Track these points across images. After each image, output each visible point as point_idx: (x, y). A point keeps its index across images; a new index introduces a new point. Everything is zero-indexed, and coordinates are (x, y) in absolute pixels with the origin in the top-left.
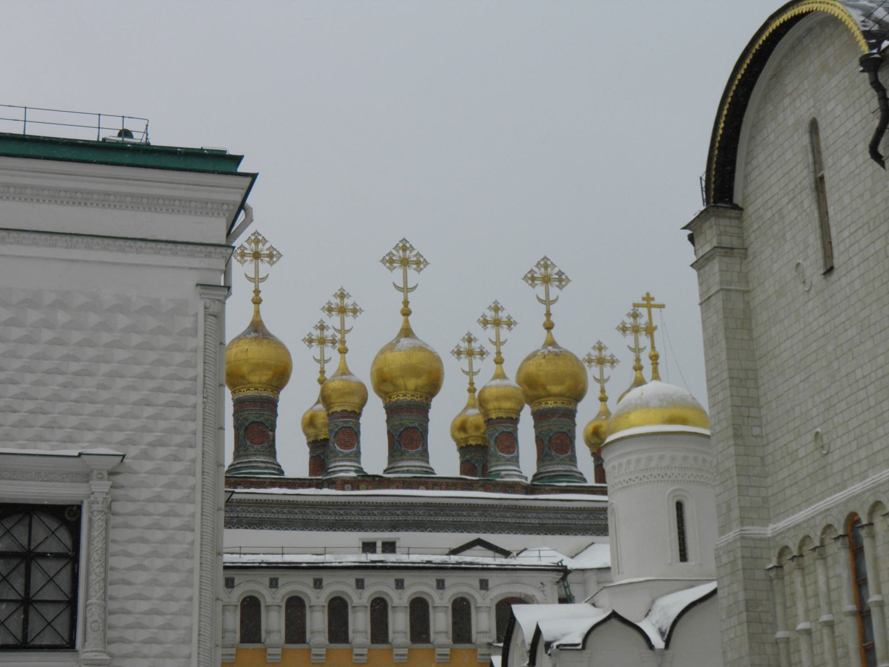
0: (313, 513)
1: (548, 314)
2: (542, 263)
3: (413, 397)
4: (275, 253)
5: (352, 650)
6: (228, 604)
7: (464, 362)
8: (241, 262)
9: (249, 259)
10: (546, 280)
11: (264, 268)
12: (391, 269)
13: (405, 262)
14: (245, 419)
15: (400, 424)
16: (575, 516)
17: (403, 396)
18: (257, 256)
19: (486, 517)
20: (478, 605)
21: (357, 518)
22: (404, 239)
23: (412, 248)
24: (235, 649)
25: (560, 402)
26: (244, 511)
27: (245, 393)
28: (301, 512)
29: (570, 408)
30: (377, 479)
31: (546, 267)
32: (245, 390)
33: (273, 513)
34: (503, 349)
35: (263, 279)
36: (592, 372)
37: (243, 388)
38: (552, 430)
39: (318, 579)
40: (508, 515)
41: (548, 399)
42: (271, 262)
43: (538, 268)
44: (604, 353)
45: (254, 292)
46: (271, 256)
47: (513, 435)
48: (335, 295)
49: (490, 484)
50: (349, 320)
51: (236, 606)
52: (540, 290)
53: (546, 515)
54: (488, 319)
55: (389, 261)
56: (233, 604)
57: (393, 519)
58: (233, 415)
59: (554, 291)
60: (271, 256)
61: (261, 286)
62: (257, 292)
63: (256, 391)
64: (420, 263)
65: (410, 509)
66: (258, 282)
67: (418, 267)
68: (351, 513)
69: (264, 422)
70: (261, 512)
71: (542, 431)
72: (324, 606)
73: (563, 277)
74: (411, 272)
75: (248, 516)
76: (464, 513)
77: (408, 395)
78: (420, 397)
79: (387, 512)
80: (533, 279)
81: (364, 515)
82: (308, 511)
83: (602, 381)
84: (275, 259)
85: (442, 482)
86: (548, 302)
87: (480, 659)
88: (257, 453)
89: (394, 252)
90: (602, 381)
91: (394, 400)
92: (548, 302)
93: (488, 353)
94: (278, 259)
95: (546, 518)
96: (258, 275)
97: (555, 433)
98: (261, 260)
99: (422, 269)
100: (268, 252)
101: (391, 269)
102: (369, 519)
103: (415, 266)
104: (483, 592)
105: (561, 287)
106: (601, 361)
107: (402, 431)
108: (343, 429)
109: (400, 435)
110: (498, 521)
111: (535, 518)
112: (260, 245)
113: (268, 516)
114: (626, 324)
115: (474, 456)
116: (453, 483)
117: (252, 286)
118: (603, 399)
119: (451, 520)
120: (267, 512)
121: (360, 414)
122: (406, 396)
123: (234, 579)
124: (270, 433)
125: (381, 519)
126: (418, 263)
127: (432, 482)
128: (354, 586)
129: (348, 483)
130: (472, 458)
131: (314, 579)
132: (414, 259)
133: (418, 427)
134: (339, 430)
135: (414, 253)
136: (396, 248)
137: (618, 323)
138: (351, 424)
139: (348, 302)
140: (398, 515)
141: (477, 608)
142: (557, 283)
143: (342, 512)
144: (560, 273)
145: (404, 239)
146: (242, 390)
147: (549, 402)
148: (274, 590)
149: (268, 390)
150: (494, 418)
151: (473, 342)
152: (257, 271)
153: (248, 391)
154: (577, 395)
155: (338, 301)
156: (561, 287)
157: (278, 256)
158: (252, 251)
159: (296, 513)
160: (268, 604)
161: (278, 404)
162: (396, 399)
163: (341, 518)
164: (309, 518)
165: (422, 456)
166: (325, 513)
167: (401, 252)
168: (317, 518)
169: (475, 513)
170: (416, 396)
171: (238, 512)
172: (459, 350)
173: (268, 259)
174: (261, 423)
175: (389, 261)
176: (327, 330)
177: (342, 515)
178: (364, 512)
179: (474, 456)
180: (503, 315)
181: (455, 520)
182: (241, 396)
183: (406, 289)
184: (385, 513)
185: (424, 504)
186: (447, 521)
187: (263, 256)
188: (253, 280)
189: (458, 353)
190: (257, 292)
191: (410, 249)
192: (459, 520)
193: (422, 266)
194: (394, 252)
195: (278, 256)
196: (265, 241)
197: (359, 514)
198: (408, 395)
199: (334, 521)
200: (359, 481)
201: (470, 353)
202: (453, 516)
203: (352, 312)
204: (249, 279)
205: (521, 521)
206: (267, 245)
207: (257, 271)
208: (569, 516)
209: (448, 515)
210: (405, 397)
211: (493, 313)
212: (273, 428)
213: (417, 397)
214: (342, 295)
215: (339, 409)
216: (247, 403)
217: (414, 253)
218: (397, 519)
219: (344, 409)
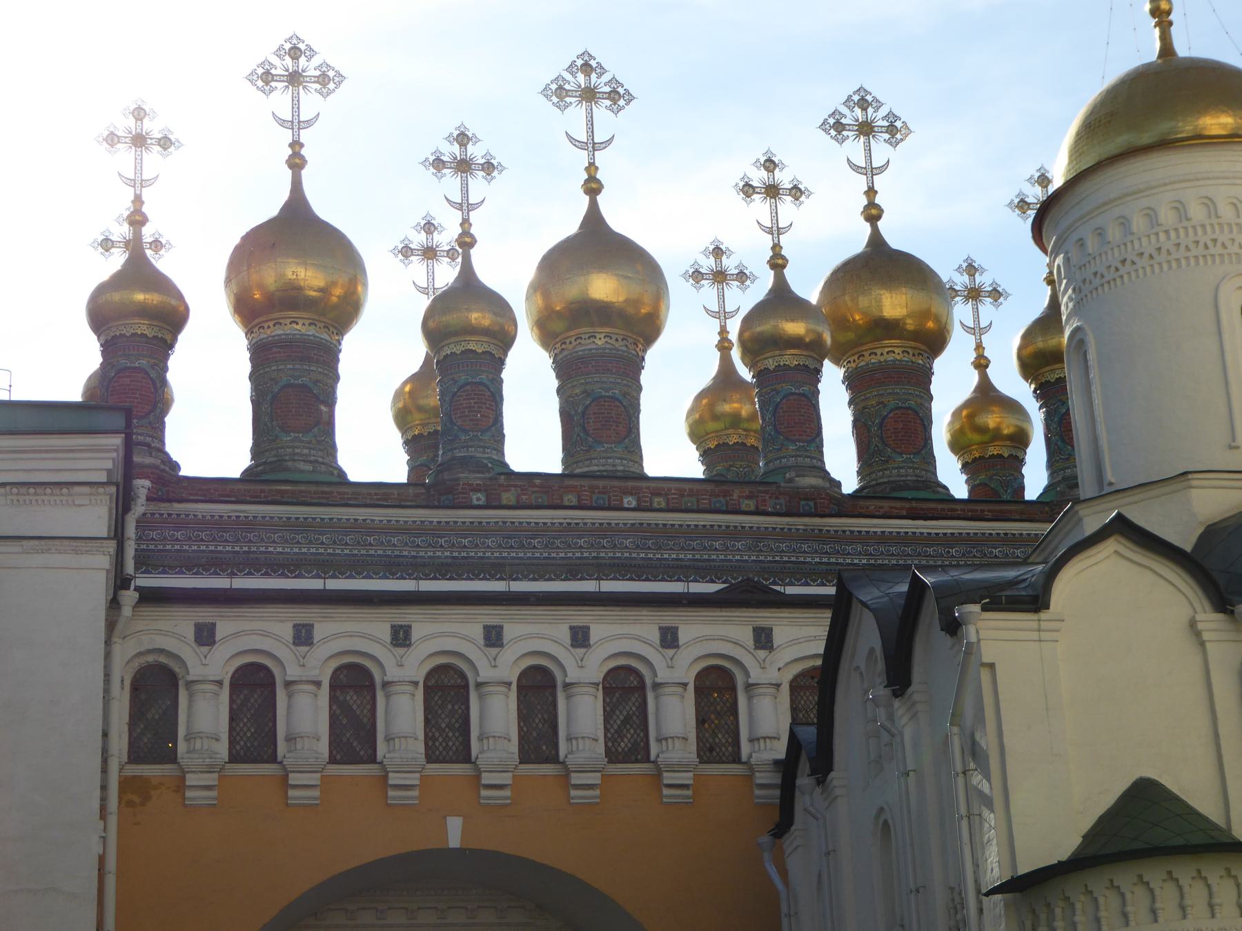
0: (406, 544)
1: (871, 192)
2: (856, 98)
3: (607, 339)
4: (331, 74)
5: (478, 777)
6: (201, 679)
7: (709, 293)
8: (263, 92)
9: (280, 85)
10: (866, 129)
11: (310, 101)
12: (563, 107)
13: (589, 95)
14: (272, 379)
15: (585, 392)
16: (941, 550)
17: (589, 338)
18: (295, 79)
19: (761, 551)
20: (751, 681)
21: (497, 554)
23: (602, 71)
24: (215, 775)
25: (897, 351)
26: (262, 540)
27: (271, 332)
28: (382, 543)
29: (920, 362)
30: (538, 482)
31: (863, 104)
32: (271, 324)
33: (322, 543)
34: (784, 240)
35: (309, 123)
36: (961, 312)
37: (267, 321)
38: (885, 406)
39: (401, 627)
40: (805, 547)
41: (876, 344)
42: (325, 91)
43: (849, 107)
44: (979, 279)
45: (291, 145)
46: (323, 79)
47: (811, 401)
48: (449, 138)
49: (766, 492)
50: (478, 185)
51: (220, 683)
52: (854, 148)
53: (882, 549)
54: (755, 184)
55: (559, 93)
56: (212, 678)
57: (570, 555)
58: (250, 378)
59: (881, 150)
60: (323, 79)
61: (305, 136)
62: (296, 145)
63: (295, 326)
64: (617, 96)
65: (605, 537)
66: (299, 129)
67: (615, 104)
68: (484, 543)
69: (311, 385)
70: (298, 542)
71: (864, 408)
72: (416, 684)
73: (898, 124)
74: (601, 112)
75: (271, 549)
76: (717, 544)
77: (598, 336)
78: (623, 340)
79: (558, 542)
80: (839, 127)
81: (512, 547)
82: (395, 540)
83: (977, 331)
84: (331, 86)
85: (670, 489)
86: (870, 171)
87: (758, 797)
88: (296, 444)
89: (568, 76)
90: (977, 331)
91: (571, 347)
92: (870, 171)
93: (754, 279)
94: (338, 84)
95: (882, 553)
96: (298, 116)
97: (891, 411)
98: (304, 87)
99: (623, 108)
100: (318, 73)
101: (563, 107)
102: (521, 555)
103: (608, 103)
104: (762, 654)
105: (894, 143)
106: (974, 294)
107: (590, 404)
108: (468, 387)
109: (584, 413)
110: (786, 559)
111: (860, 554)
112: (303, 60)
113: (313, 550)
114: (1028, 196)
115: (732, 466)
116: (691, 490)
117: (287, 136)
118: (981, 364)
119: (690, 557)
120: (311, 542)
121: (500, 363)
122: (595, 338)
123: (214, 625)
124: (323, 408)
125: (546, 555)
126: (614, 96)
127: (648, 488)
128: (481, 642)
129: (479, 491)
130: (728, 470)
131: (392, 627)
132: (607, 89)
133: (620, 397)
134: (458, 390)
135: (606, 78)
136: (571, 68)
137: (1011, 195)
138: (483, 377)
140: (581, 547)
141: (749, 687)
142: (887, 136)
143: (466, 542)
144: (892, 117)
146: (266, 325)
147: (879, 351)
148: (304, 649)
149: (319, 325)
150: (772, 368)
151: (724, 258)
152: (296, 105)
153: (277, 326)
154: (935, 342)
155: (456, 149)
156: (894, 143)
157: (337, 79)
158: (287, 70)
159: (370, 544)
160: (288, 678)
161: (341, 356)
162: (574, 343)
163: (464, 554)
164: (397, 553)
165: (629, 452)
166: (430, 545)
168: (413, 554)
169: (739, 545)
170: (614, 337)
171: (250, 541)
172: (697, 271)
173: (318, 86)
174: (303, 386)
175: (559, 93)
176: (440, 233)
177: (465, 547)
178: (512, 542)
179: (732, 466)
180: (783, 178)
181: (698, 557)
182: (263, 336)
183: (592, 146)
184: (553, 543)
185: (633, 525)
186: (681, 560)
187: (308, 79)
189: (697, 276)
190: (296, 145)
191: (598, 71)
192: (706, 557)
193: (622, 102)
194: (568, 76)
195: (337, 79)
196: (311, 52)
197: (500, 546)
198: (598, 336)
199: (450, 561)
200: (500, 486)
201: (720, 277)
202: (694, 549)
203: (483, 170)
204: (282, 123)
205: (833, 560)
206: (316, 61)
207: (296, 105)
208: (930, 550)
209: (682, 548)
210: (592, 339)
211: (763, 174)
212: (329, 399)
213: (617, 340)
214: (463, 139)
215: (458, 349)
216: (275, 350)
217: (606, 78)
218: (578, 555)
219: (468, 347)
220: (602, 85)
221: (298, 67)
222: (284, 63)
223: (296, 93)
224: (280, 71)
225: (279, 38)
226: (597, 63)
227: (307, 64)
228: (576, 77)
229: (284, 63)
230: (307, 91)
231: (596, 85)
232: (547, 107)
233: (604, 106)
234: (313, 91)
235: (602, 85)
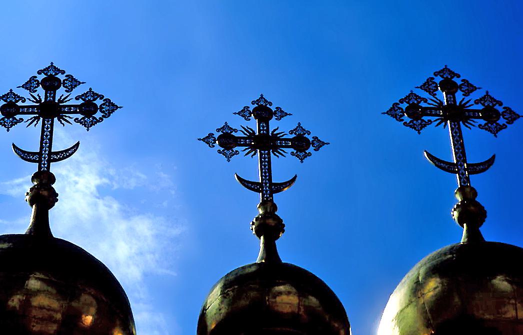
4: (99, 102)
9: (26, 117)
22: (446, 69)
23: (469, 88)
48: (244, 113)
74: (473, 133)
89: (424, 94)
94: (107, 115)
99: (504, 127)
100: (80, 102)
112: (61, 92)
132: (480, 107)
139: (279, 127)
145: (446, 69)
152: (47, 137)
155: (254, 125)
157: (105, 108)
167: (443, 96)
173: (80, 116)
188: (36, 157)
193: (502, 121)
196: (73, 83)
204: (26, 156)
206: (79, 91)
214: (263, 112)
220: (472, 102)
221: (54, 98)
222: (35, 94)
223: (48, 125)
224: (28, 103)
225: (32, 68)
226: (462, 81)
227: (66, 94)
228: (435, 94)
229: (35, 94)
230: (63, 122)
231: (463, 102)
232: (398, 129)
233: (477, 125)
234: (72, 121)
235: (472, 102)
